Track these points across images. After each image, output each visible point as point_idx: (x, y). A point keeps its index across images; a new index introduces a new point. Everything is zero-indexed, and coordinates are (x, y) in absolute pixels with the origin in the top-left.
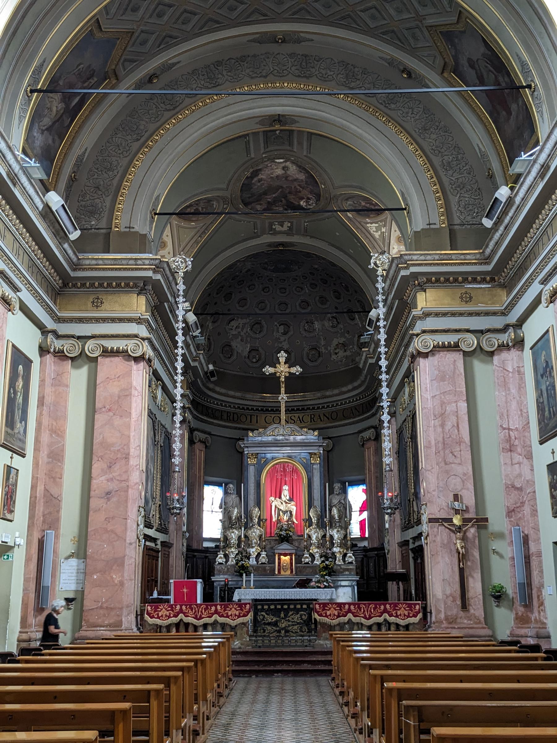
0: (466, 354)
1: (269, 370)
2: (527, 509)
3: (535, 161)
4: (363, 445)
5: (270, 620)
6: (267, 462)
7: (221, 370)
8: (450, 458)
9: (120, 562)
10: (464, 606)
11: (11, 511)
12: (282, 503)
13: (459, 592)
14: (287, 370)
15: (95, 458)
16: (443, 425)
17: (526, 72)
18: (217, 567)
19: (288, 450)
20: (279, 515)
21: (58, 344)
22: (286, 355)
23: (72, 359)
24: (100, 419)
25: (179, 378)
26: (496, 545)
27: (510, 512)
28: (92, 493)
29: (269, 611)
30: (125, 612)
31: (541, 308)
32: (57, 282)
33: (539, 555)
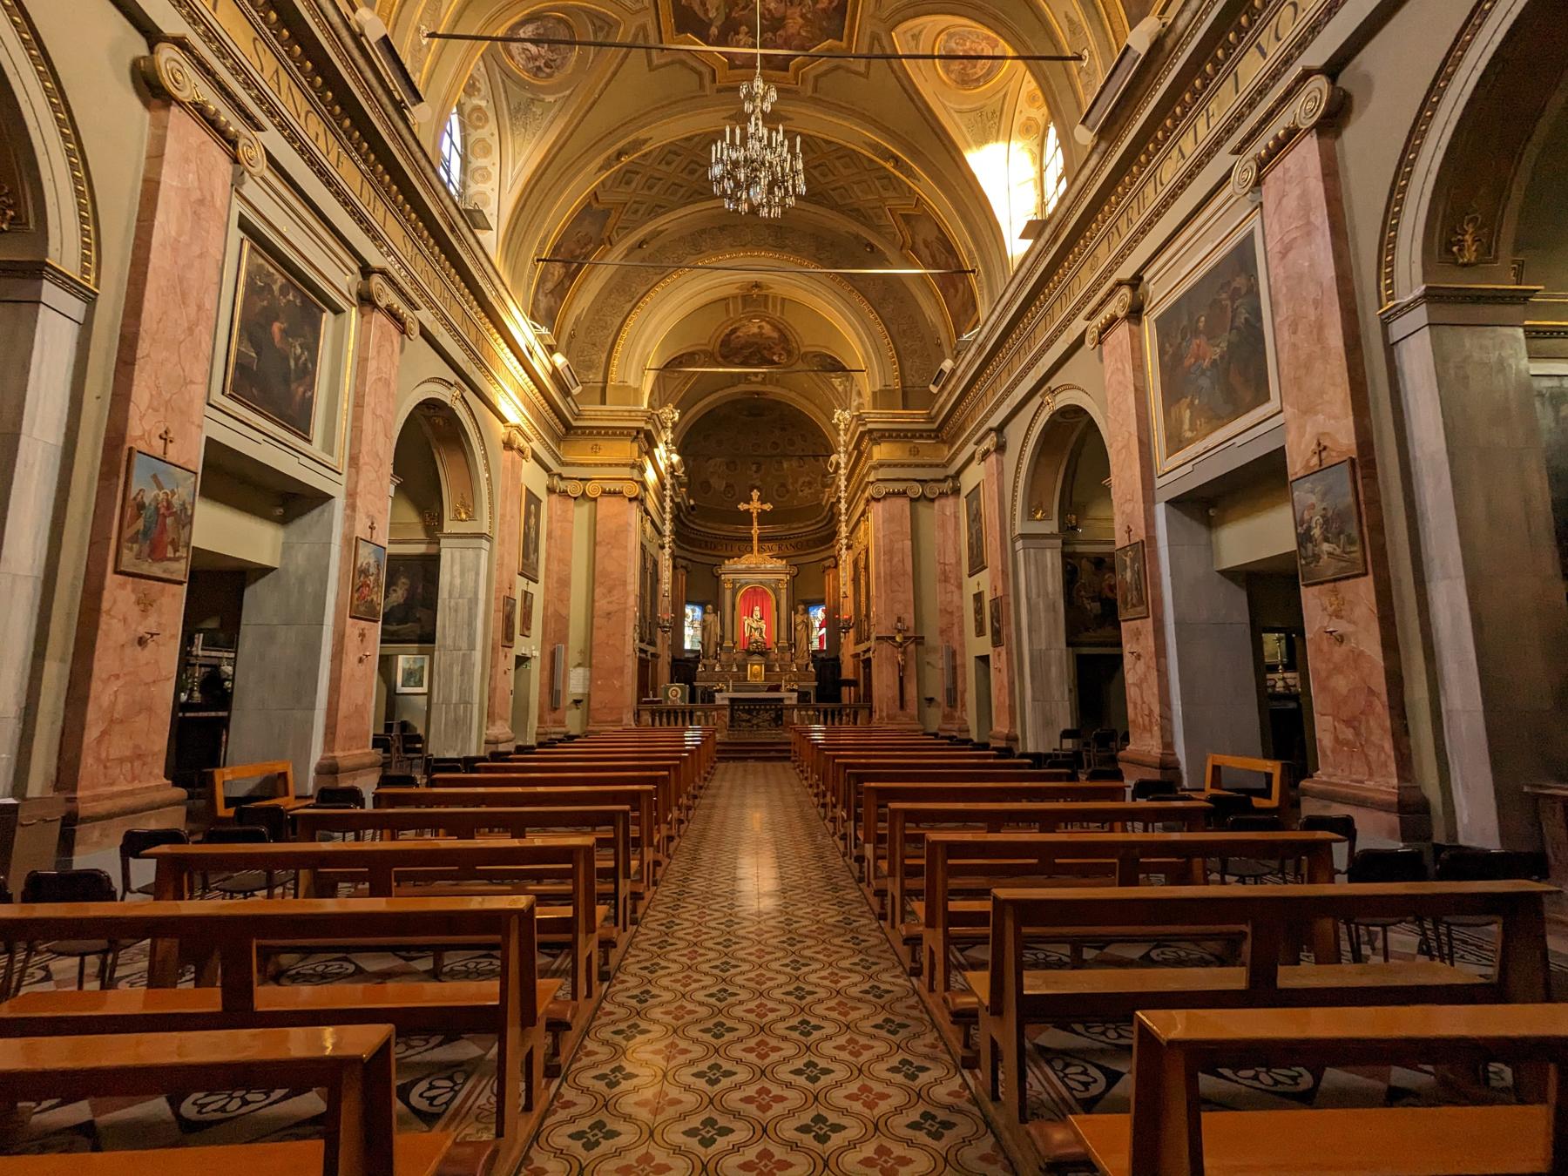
0: (912, 500)
1: (742, 506)
2: (956, 630)
3: (975, 340)
6: (741, 587)
8: (896, 587)
9: (620, 671)
10: (902, 707)
11: (529, 629)
13: (898, 697)
15: (597, 585)
16: (891, 560)
17: (972, 259)
19: (760, 577)
21: (562, 485)
23: (575, 498)
24: (600, 550)
25: (668, 516)
26: (932, 658)
27: (942, 632)
28: (596, 614)
29: (744, 711)
30: (625, 711)
31: (975, 463)
32: (561, 429)
33: (964, 666)
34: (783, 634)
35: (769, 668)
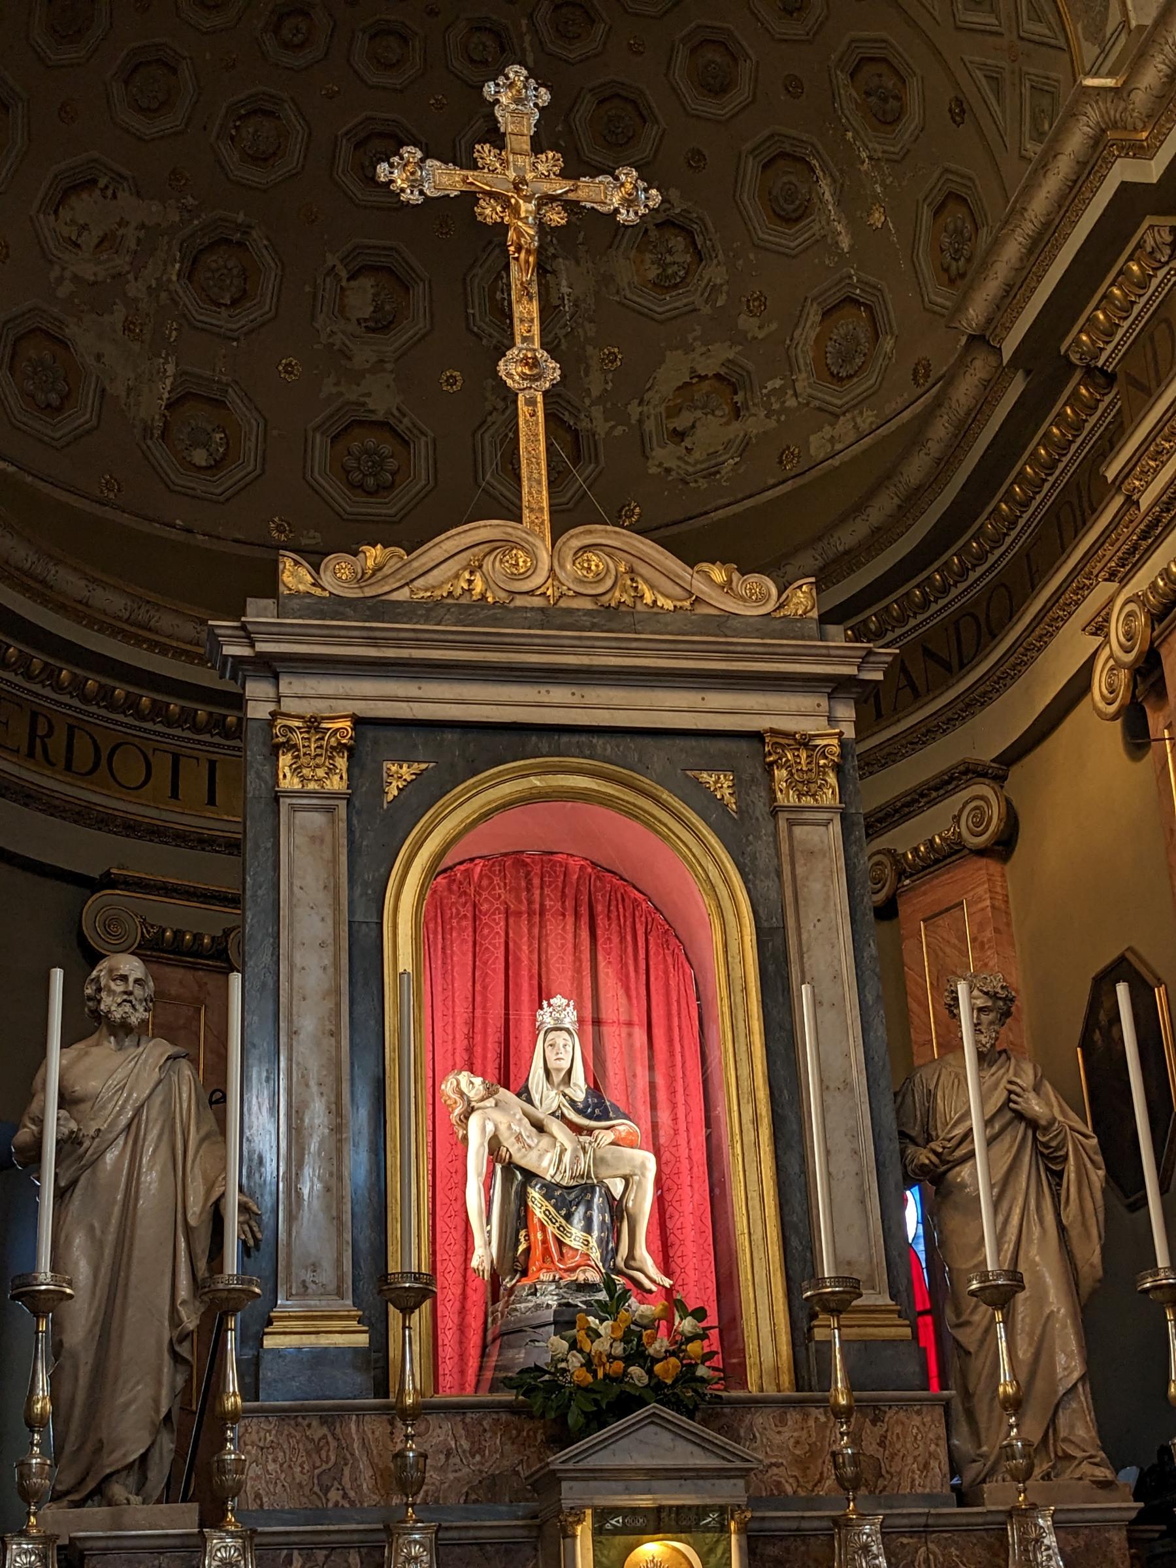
12: (540, 1127)
14: (559, 188)
22: (545, 96)
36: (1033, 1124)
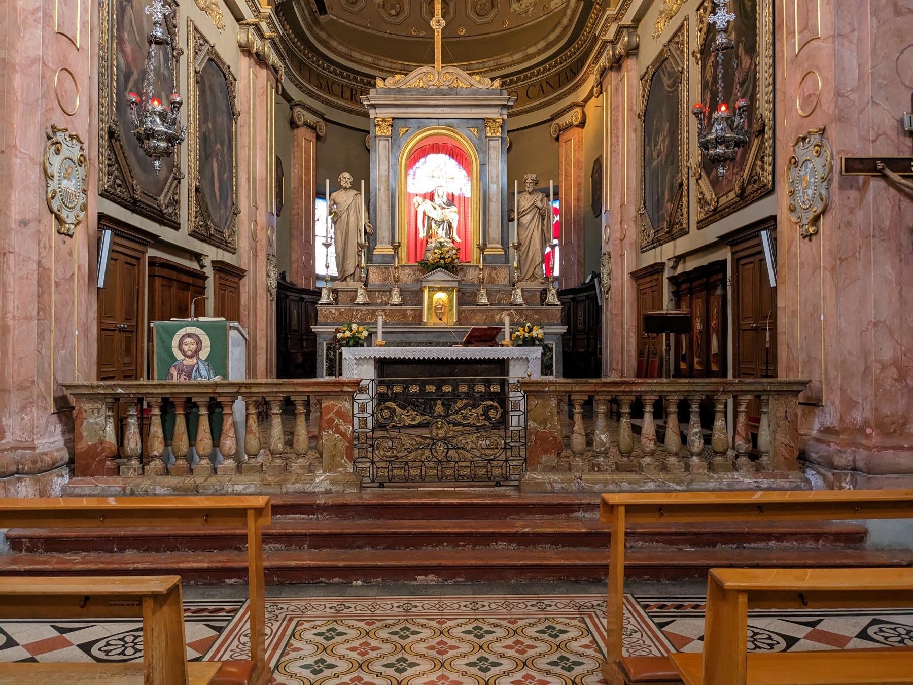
4: (557, 139)
5: (408, 421)
7: (341, 21)
12: (435, 208)
18: (322, 311)
20: (430, 227)
34: (495, 232)
35: (466, 298)
36: (538, 208)
